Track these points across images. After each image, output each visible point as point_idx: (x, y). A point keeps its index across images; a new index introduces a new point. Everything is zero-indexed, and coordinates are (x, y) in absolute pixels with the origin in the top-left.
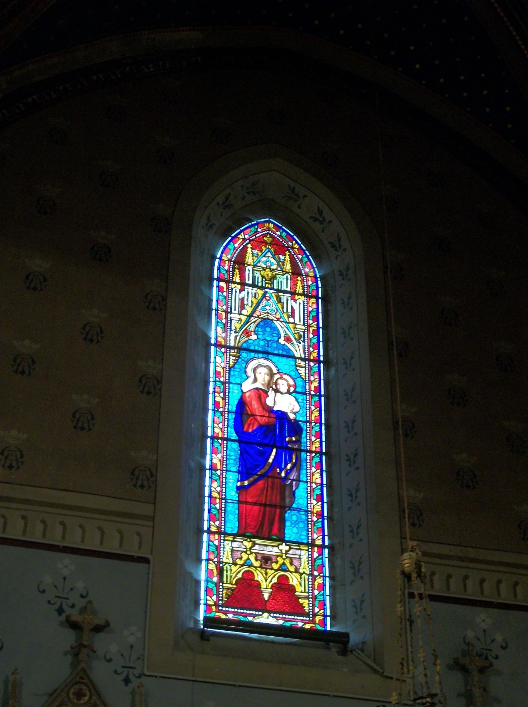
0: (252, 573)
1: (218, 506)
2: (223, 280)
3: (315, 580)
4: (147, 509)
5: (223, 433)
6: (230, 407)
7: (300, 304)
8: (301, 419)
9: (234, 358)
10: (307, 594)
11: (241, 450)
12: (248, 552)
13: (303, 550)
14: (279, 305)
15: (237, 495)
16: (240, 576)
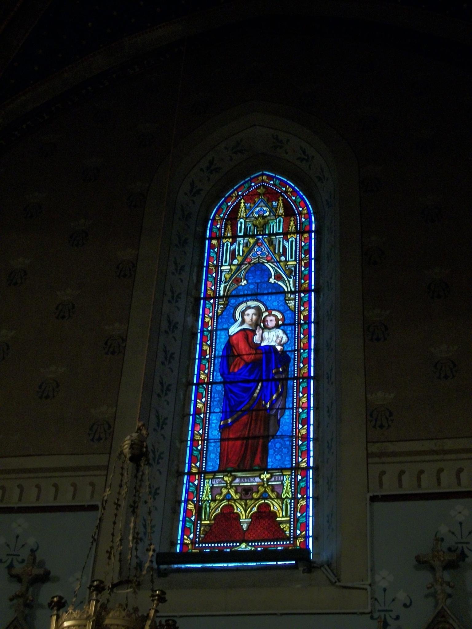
0: (232, 506)
1: (199, 448)
3: (298, 503)
4: (102, 460)
5: (209, 378)
6: (217, 353)
8: (290, 349)
9: (222, 306)
10: (288, 519)
11: (225, 391)
13: (286, 475)
14: (271, 248)
15: (220, 434)
16: (218, 511)
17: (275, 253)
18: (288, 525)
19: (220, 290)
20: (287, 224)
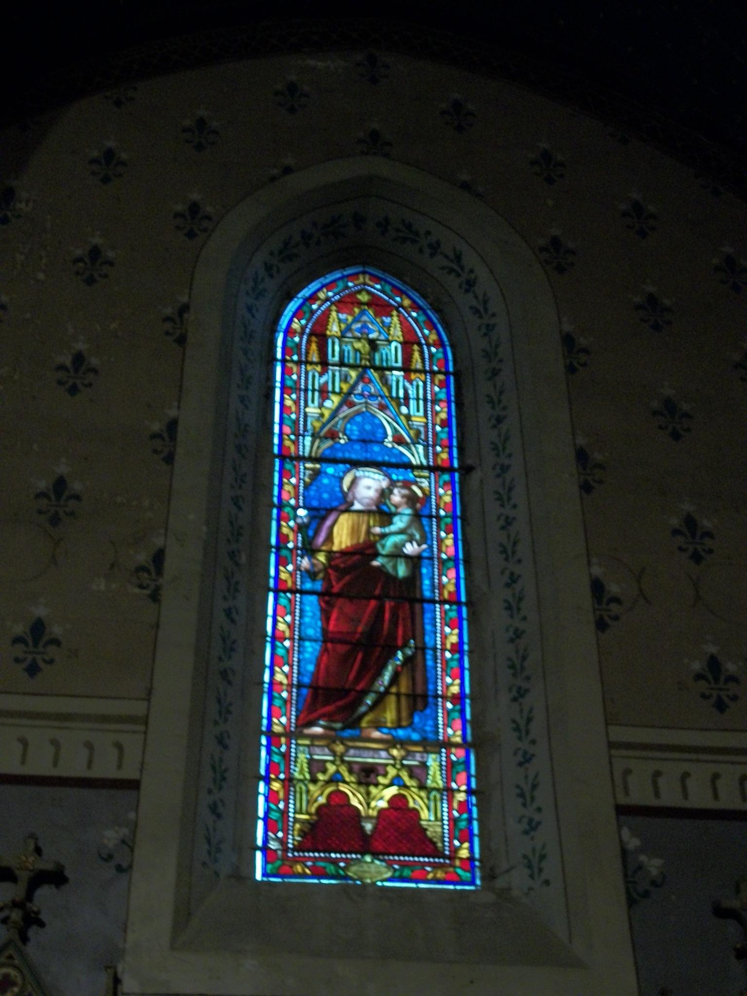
12: (338, 763)
19: (304, 446)
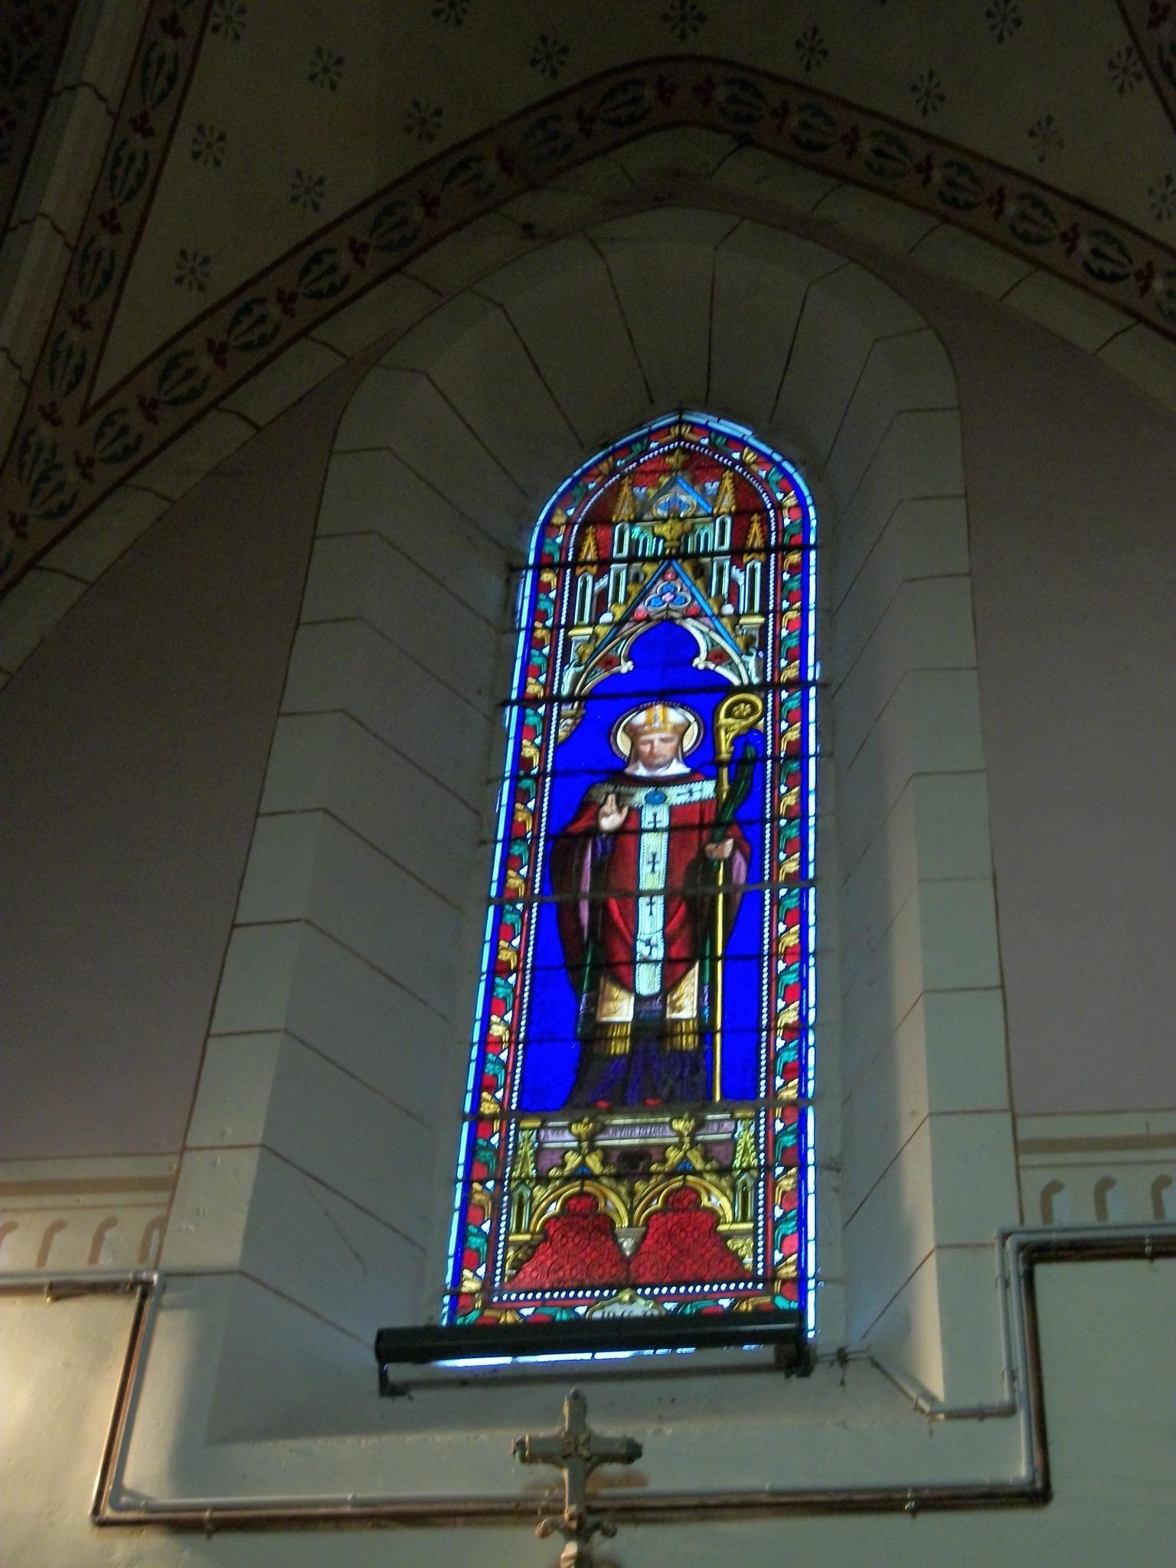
2: (552, 566)
7: (753, 570)
14: (699, 583)
17: (709, 596)
18: (749, 1240)
19: (561, 683)
20: (741, 531)
